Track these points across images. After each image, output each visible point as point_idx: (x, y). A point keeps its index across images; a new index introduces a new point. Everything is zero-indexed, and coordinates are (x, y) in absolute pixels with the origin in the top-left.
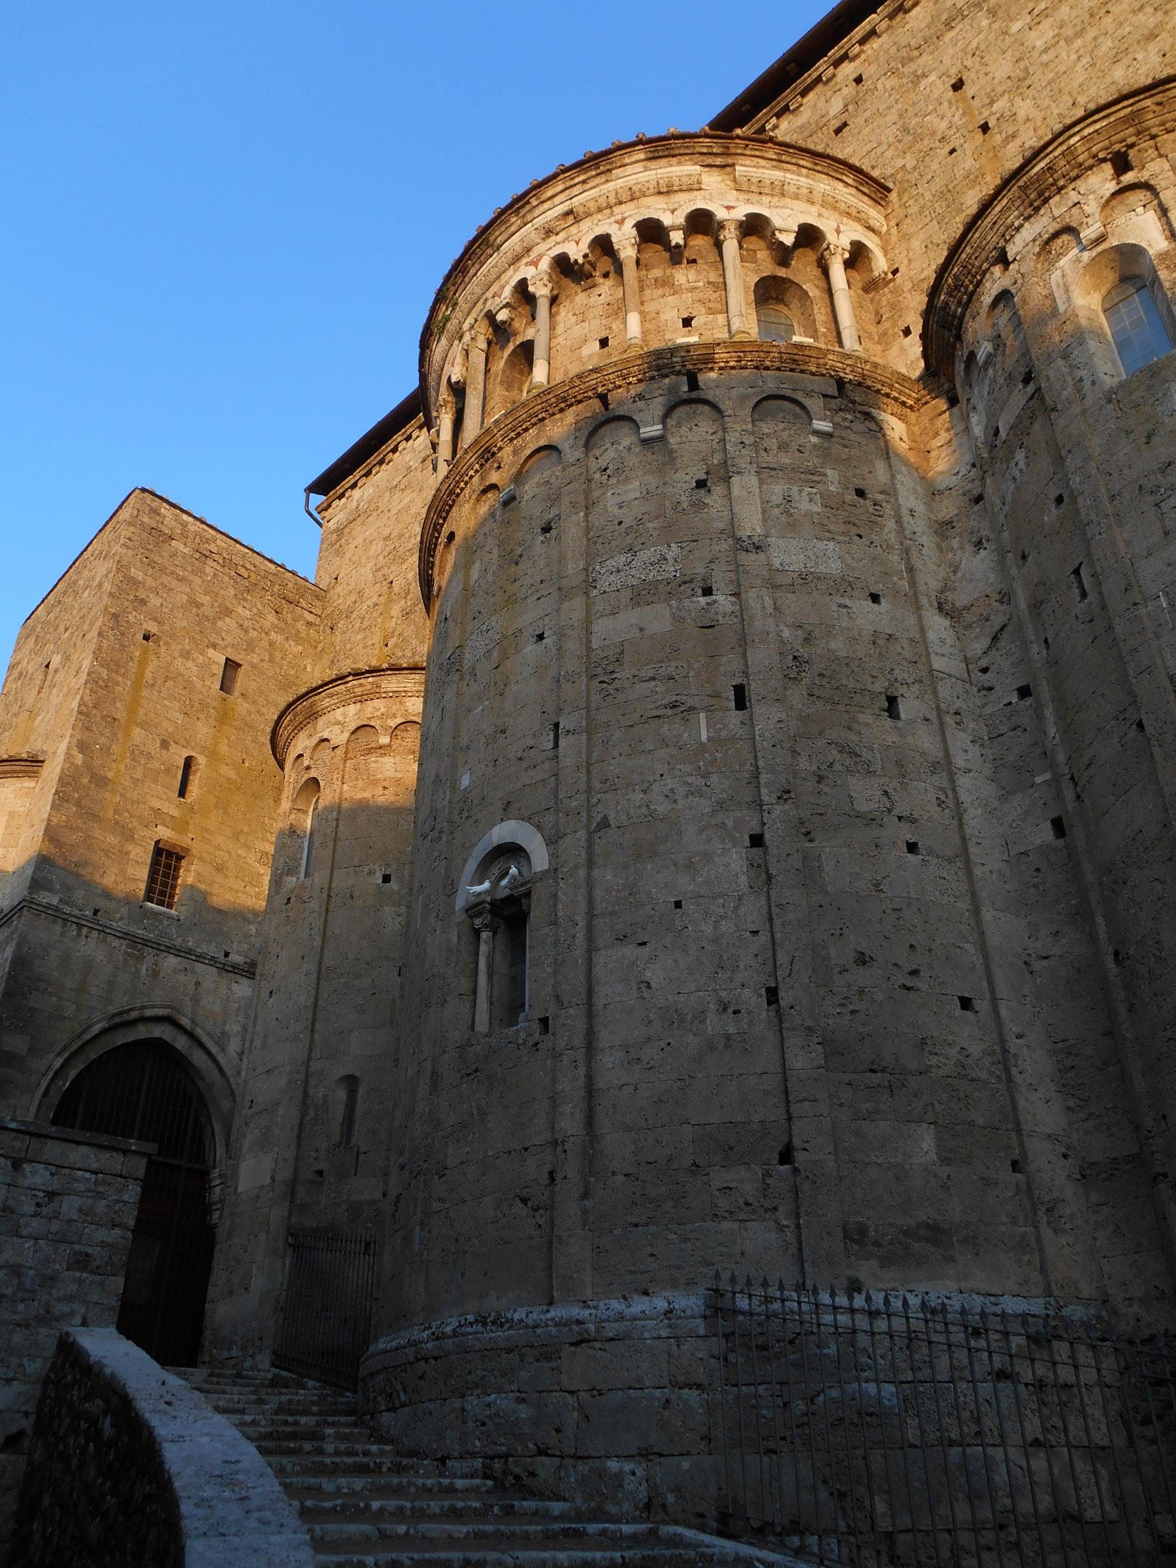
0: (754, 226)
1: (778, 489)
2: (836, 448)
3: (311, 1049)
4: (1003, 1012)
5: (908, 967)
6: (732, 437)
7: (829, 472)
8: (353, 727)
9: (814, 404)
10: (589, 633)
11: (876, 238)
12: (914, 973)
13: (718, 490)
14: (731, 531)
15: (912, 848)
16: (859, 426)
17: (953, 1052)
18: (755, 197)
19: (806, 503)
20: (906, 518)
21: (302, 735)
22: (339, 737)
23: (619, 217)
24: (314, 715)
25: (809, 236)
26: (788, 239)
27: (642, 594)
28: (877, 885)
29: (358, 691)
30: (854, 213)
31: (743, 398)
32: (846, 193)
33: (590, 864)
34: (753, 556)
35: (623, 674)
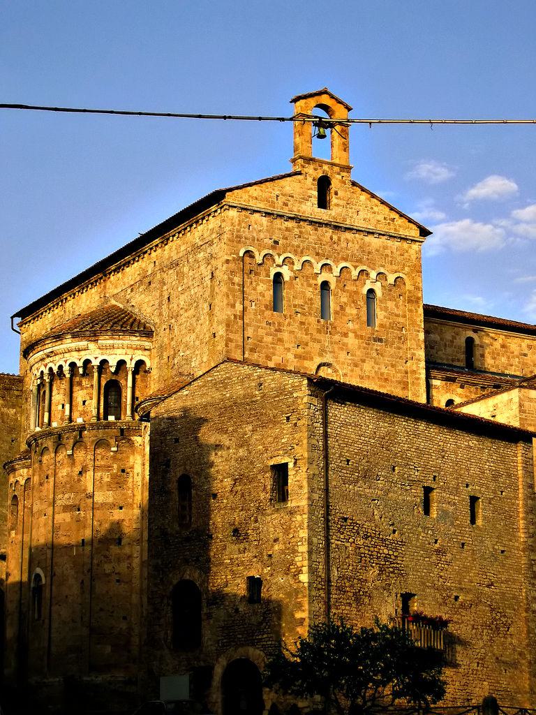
0: (104, 362)
1: (98, 475)
2: (119, 456)
3: (21, 596)
4: (132, 619)
5: (111, 611)
6: (89, 457)
7: (115, 466)
8: (26, 478)
9: (112, 441)
10: (53, 518)
11: (147, 353)
12: (113, 612)
13: (84, 475)
14: (85, 490)
15: (118, 581)
16: (127, 444)
17: (118, 629)
18: (104, 351)
19: (106, 479)
20: (135, 476)
21: (11, 476)
22: (22, 482)
23: (65, 359)
24: (14, 470)
25: (121, 364)
26: (113, 370)
27: (66, 508)
28: (107, 592)
29: (27, 464)
30: (138, 347)
31: (93, 441)
32: (135, 340)
33: (51, 585)
34: (89, 500)
35: (60, 533)
